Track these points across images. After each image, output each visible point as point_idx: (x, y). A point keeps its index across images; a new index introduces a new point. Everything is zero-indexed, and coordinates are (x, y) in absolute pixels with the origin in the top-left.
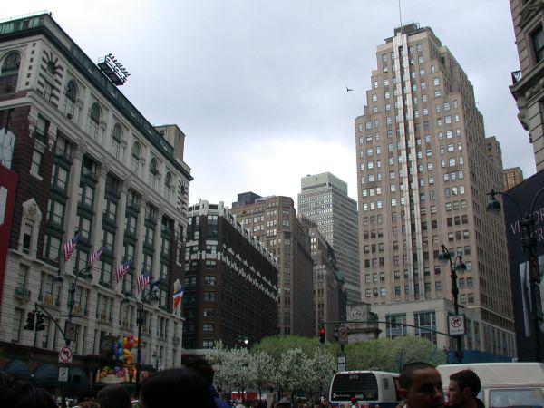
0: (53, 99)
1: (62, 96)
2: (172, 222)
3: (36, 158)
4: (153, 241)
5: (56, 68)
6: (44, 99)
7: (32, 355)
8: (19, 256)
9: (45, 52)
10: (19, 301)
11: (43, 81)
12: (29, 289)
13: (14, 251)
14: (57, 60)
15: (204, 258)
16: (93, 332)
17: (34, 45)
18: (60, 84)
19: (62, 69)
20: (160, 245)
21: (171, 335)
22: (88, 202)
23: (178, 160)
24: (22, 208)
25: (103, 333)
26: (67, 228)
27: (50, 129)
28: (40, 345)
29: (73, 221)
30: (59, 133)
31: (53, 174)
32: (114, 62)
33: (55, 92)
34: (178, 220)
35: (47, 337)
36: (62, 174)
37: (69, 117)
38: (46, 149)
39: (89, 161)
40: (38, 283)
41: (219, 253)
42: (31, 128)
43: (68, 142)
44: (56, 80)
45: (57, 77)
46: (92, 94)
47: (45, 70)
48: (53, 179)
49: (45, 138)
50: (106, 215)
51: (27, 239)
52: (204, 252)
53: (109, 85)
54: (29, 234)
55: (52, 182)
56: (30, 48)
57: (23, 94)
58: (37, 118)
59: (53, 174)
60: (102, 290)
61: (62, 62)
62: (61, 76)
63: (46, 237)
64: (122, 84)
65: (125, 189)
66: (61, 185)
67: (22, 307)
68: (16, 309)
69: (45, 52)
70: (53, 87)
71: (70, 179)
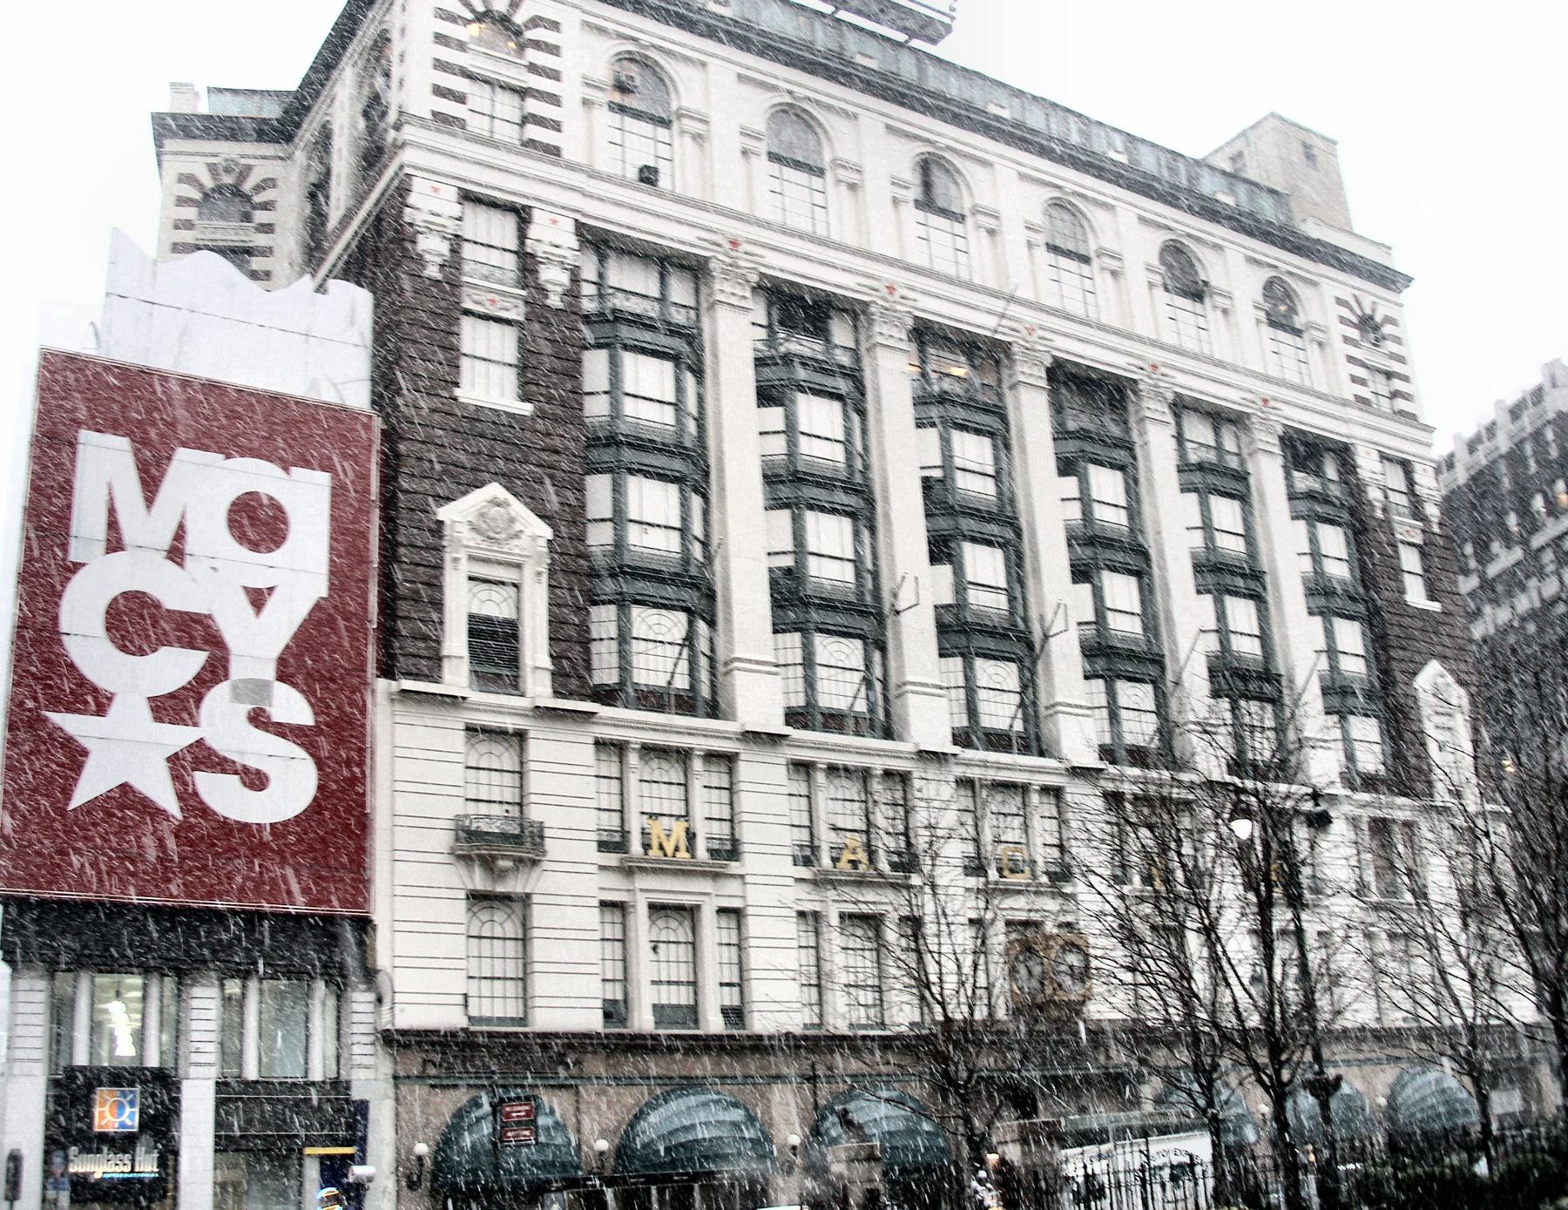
0: (533, 132)
2: (1344, 454)
6: (490, 143)
7: (596, 1065)
8: (454, 702)
12: (535, 814)
16: (965, 937)
18: (554, 75)
19: (555, 26)
20: (1290, 548)
23: (1312, 230)
24: (438, 529)
27: (533, 232)
28: (643, 1021)
30: (597, 241)
33: (533, 106)
35: (694, 984)
37: (648, 176)
42: (432, 247)
43: (665, 261)
44: (533, 68)
45: (532, 55)
49: (527, 264)
55: (596, 409)
58: (456, 210)
60: (969, 764)
62: (554, 50)
65: (1029, 375)
67: (500, 889)
68: (477, 898)
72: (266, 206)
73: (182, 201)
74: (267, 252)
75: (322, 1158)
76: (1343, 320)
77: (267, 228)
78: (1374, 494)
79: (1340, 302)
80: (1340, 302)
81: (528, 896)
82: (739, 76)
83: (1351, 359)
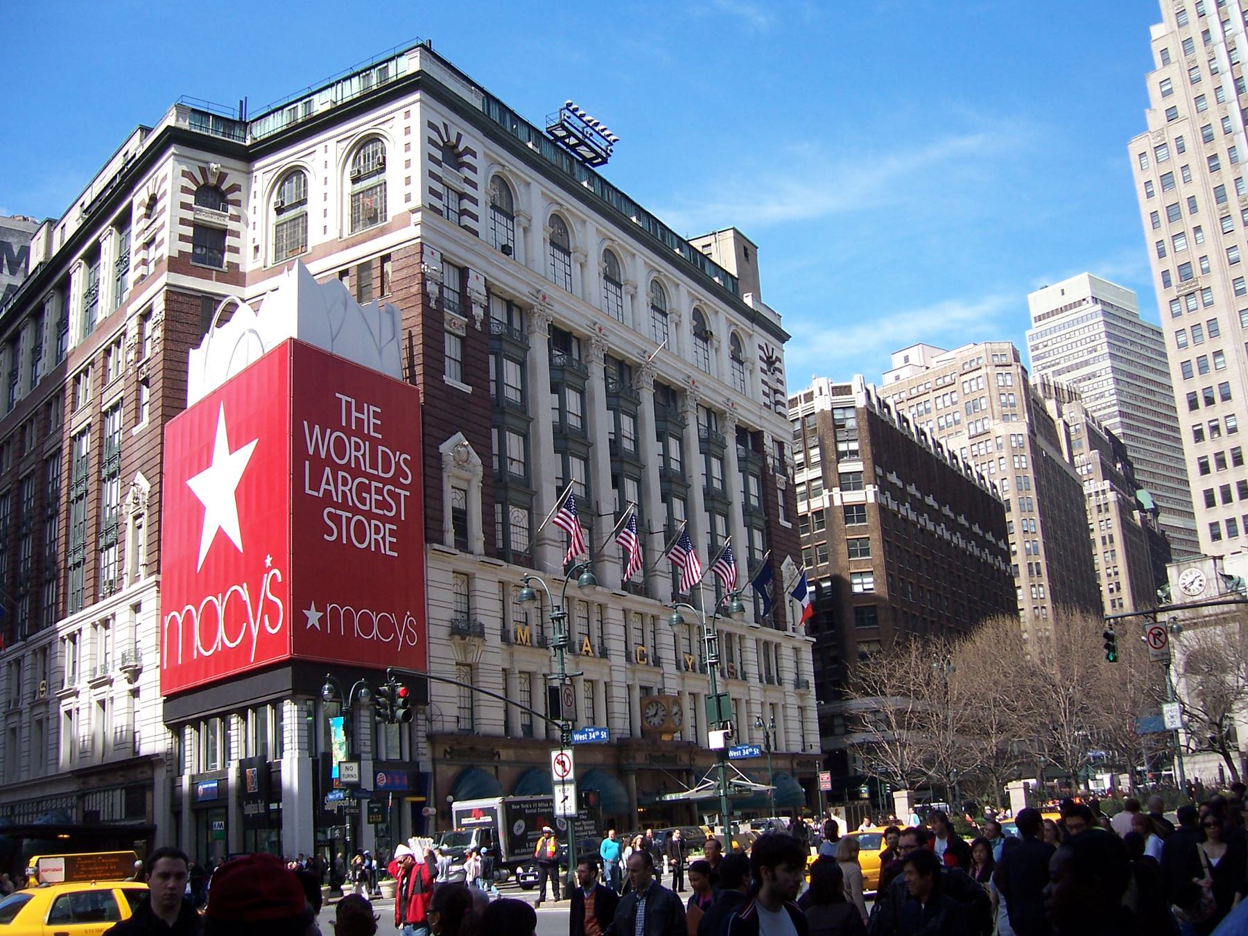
1: (482, 210)
2: (758, 436)
3: (452, 348)
4: (723, 481)
5: (460, 155)
9: (431, 126)
11: (439, 187)
13: (436, 546)
14: (459, 136)
15: (837, 502)
17: (407, 114)
18: (474, 185)
19: (474, 155)
21: (789, 676)
22: (574, 421)
25: (646, 690)
26: (540, 486)
29: (548, 463)
31: (493, 376)
32: (580, 117)
33: (466, 204)
34: (771, 428)
36: (511, 373)
38: (470, 327)
39: (561, 338)
40: (497, 606)
44: (467, 180)
45: (467, 172)
46: (543, 194)
47: (438, 163)
48: (493, 385)
49: (465, 304)
50: (615, 444)
51: (461, 517)
52: (836, 490)
53: (576, 167)
54: (463, 507)
56: (399, 121)
57: (403, 222)
59: (493, 376)
61: (472, 139)
62: (474, 170)
63: (498, 508)
64: (605, 161)
66: (512, 395)
67: (469, 661)
69: (431, 126)
70: (462, 196)
71: (531, 379)
72: (237, 203)
73: (185, 190)
74: (236, 234)
75: (413, 803)
76: (761, 358)
77: (237, 218)
78: (770, 461)
79: (761, 347)
80: (761, 347)
82: (543, 194)
83: (763, 382)
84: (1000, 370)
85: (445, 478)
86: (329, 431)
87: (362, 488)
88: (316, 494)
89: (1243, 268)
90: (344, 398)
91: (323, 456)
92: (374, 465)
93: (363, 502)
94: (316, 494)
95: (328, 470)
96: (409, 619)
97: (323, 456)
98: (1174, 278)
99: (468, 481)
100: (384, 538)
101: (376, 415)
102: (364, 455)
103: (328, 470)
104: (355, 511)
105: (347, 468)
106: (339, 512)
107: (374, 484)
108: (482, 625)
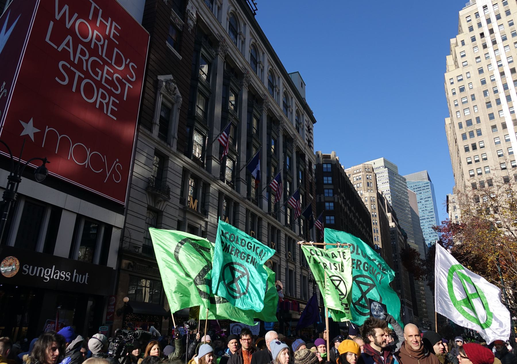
8: (153, 139)
10: (155, 198)
15: (322, 200)
27: (189, 7)
41: (336, 195)
67: (157, 207)
81: (163, 211)
84: (367, 174)
85: (158, 94)
86: (76, 15)
87: (95, 64)
88: (56, 47)
89: (496, 121)
90: (94, 4)
91: (68, 26)
92: (109, 54)
93: (97, 74)
94: (56, 47)
95: (69, 38)
96: (116, 163)
97: (68, 26)
98: (464, 125)
99: (173, 104)
100: (108, 104)
101: (116, 28)
102: (103, 46)
103: (69, 38)
104: (87, 75)
105: (87, 45)
106: (72, 68)
107: (106, 67)
108: (169, 188)
